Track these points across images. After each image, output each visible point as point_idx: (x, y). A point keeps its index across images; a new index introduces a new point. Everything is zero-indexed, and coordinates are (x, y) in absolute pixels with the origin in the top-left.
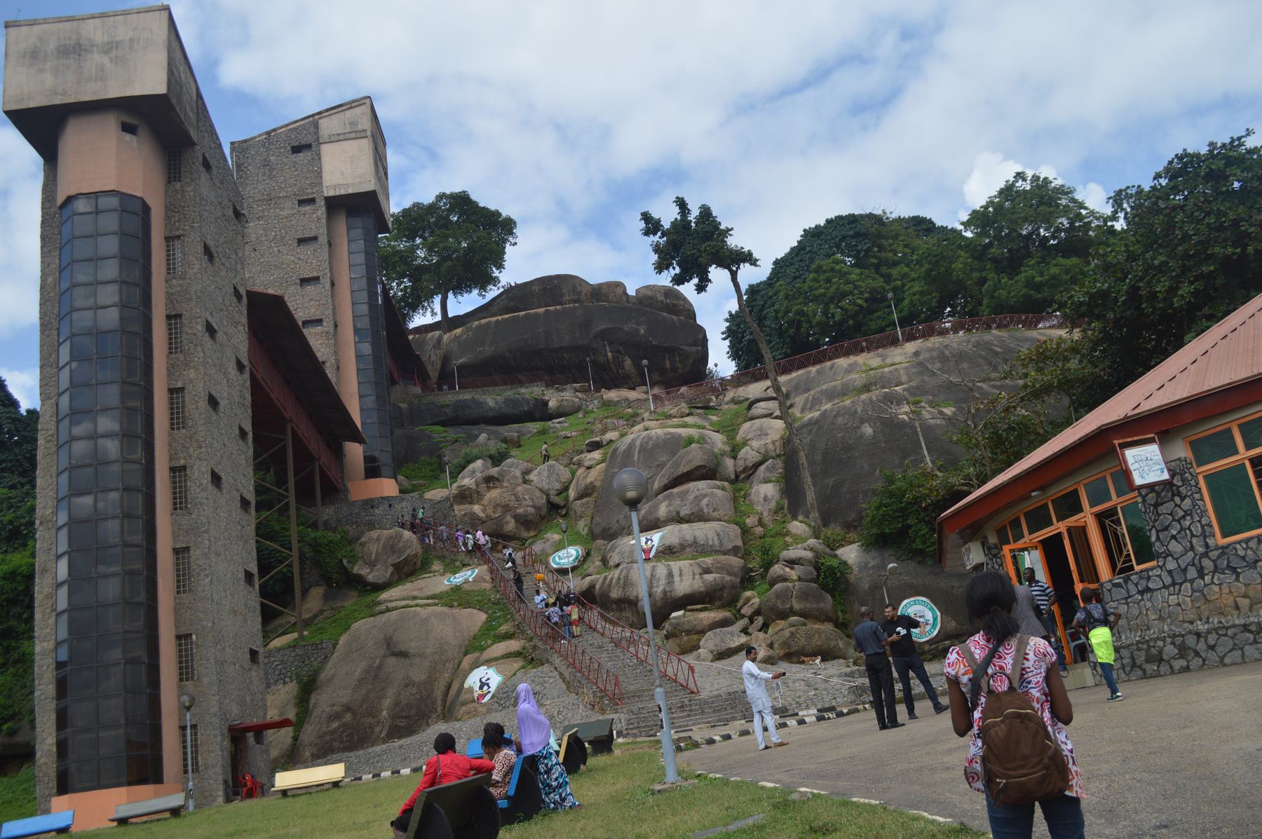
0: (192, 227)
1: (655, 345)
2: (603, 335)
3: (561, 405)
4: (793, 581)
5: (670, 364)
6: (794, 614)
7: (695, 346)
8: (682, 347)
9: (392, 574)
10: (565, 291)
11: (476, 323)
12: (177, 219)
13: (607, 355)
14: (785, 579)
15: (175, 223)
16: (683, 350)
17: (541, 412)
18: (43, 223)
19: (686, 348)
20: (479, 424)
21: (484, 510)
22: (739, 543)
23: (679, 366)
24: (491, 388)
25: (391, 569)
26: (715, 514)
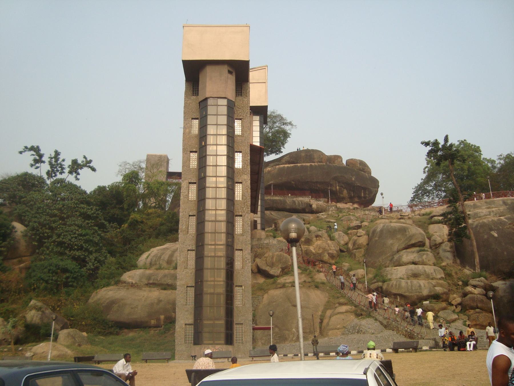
0: (247, 116)
1: (358, 186)
2: (335, 179)
4: (475, 294)
5: (363, 195)
6: (478, 308)
9: (280, 272)
11: (277, 166)
12: (240, 111)
13: (336, 187)
14: (471, 293)
15: (239, 113)
17: (308, 210)
18: (185, 107)
19: (371, 188)
21: (315, 249)
22: (443, 276)
25: (280, 270)
26: (428, 262)
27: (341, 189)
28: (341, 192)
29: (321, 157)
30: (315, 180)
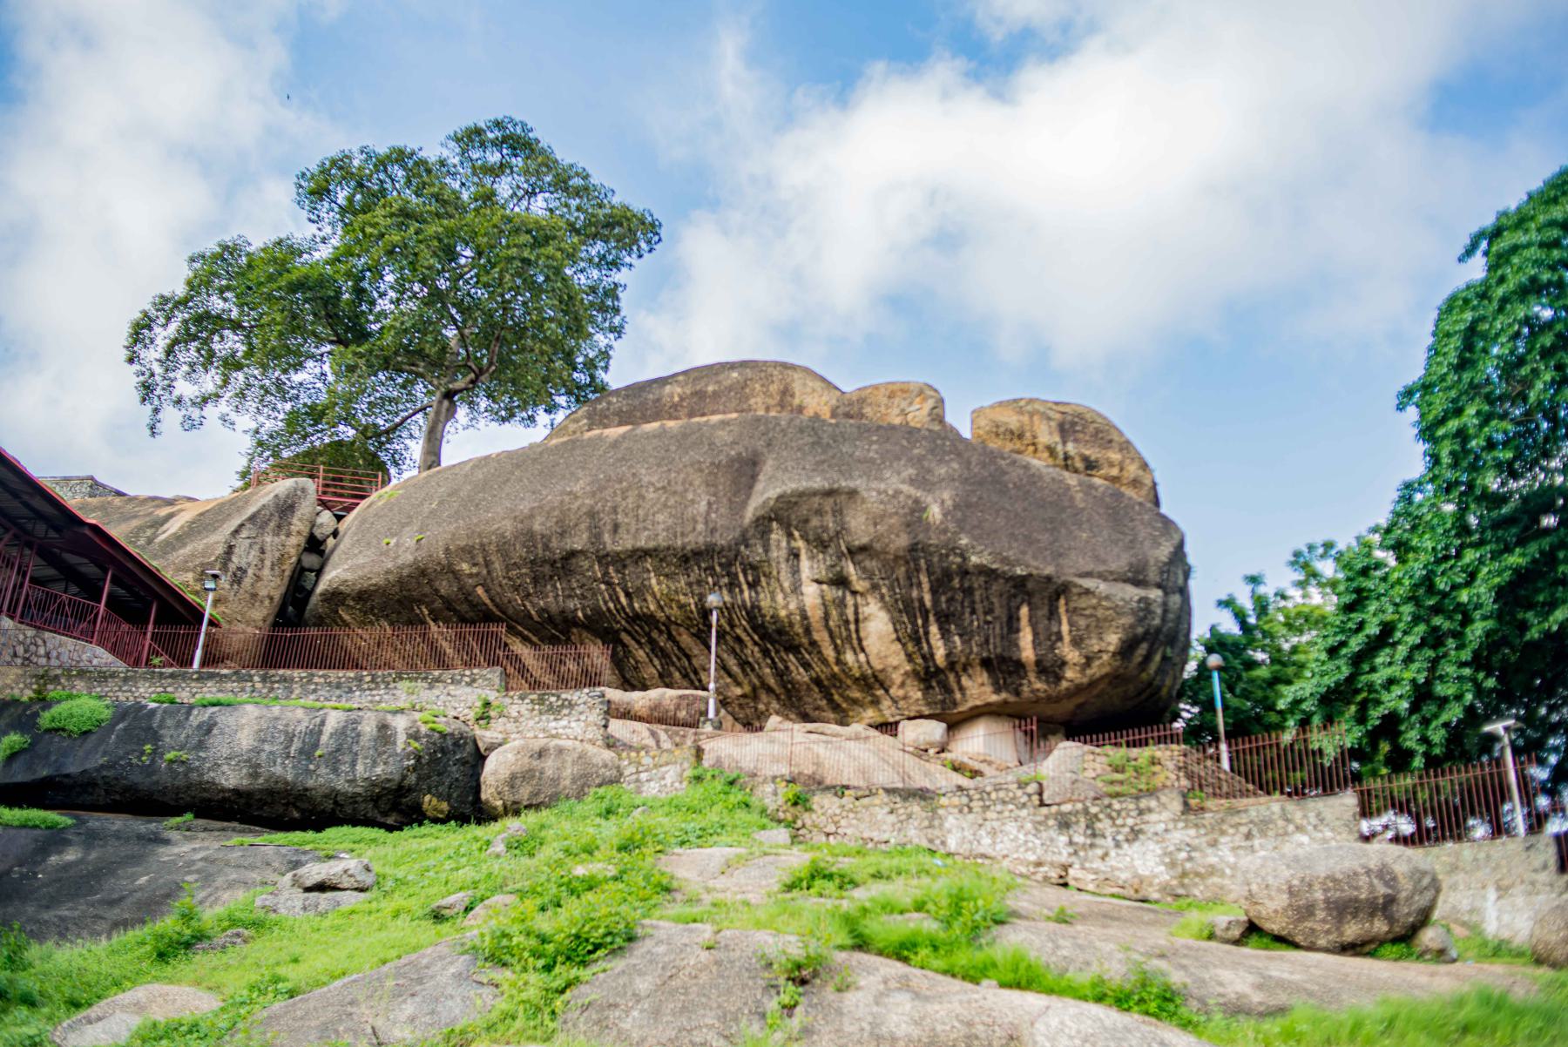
1: (983, 571)
3: (528, 775)
7: (1138, 583)
8: (1088, 583)
13: (796, 589)
16: (1088, 592)
20: (178, 812)
24: (297, 673)
27: (841, 604)
28: (849, 633)
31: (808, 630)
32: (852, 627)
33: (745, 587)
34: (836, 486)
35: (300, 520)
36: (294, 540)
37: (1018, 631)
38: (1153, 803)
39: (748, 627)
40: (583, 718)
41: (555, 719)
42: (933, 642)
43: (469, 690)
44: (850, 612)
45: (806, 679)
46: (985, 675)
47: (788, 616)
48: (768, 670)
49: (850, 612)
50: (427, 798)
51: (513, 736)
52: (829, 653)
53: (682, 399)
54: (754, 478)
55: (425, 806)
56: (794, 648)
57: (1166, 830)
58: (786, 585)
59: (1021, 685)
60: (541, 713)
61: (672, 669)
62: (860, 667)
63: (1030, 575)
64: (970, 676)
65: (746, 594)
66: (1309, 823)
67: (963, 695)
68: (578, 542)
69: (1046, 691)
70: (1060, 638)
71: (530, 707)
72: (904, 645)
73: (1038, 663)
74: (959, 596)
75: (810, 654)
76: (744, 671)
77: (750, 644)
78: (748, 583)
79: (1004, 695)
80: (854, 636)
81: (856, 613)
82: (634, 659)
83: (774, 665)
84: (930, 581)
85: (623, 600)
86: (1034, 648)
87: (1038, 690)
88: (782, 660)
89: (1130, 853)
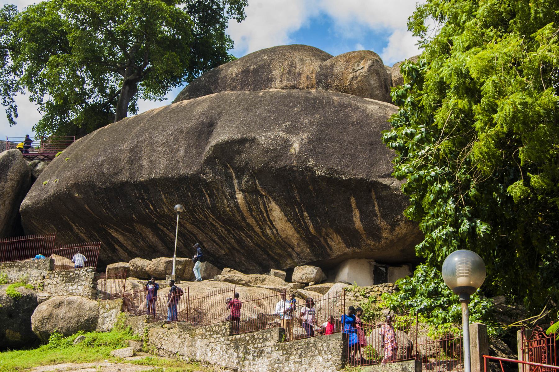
8: (386, 181)
10: (276, 73)
16: (386, 187)
23: (384, 224)
27: (256, 203)
29: (297, 70)
30: (144, 176)
31: (244, 219)
32: (265, 214)
33: (207, 196)
34: (250, 135)
35: (11, 172)
36: (9, 184)
37: (352, 211)
38: (269, 335)
39: (214, 218)
40: (83, 283)
41: (72, 285)
42: (306, 221)
43: (36, 271)
44: (262, 206)
45: (252, 244)
46: (339, 237)
47: (230, 211)
48: (233, 240)
49: (262, 206)
50: (7, 331)
51: (53, 295)
52: (258, 229)
53: (237, 76)
54: (210, 134)
55: (7, 335)
56: (240, 228)
57: (272, 351)
58: (227, 194)
59: (360, 242)
60: (66, 282)
61: (189, 242)
62: (275, 237)
63: (350, 179)
64: (331, 239)
65: (208, 200)
66: (323, 350)
67: (331, 249)
68: (124, 177)
69: (374, 245)
70: (376, 215)
71: (61, 278)
72: (292, 224)
73: (365, 229)
74: (314, 194)
75: (249, 231)
76: (222, 241)
77: (219, 226)
78: (208, 194)
79: (352, 249)
80: (267, 220)
81: (265, 207)
82: (170, 237)
83: (235, 238)
84: (296, 187)
85: (151, 207)
86: (361, 221)
87: (370, 245)
88: (238, 235)
89: (258, 363)
